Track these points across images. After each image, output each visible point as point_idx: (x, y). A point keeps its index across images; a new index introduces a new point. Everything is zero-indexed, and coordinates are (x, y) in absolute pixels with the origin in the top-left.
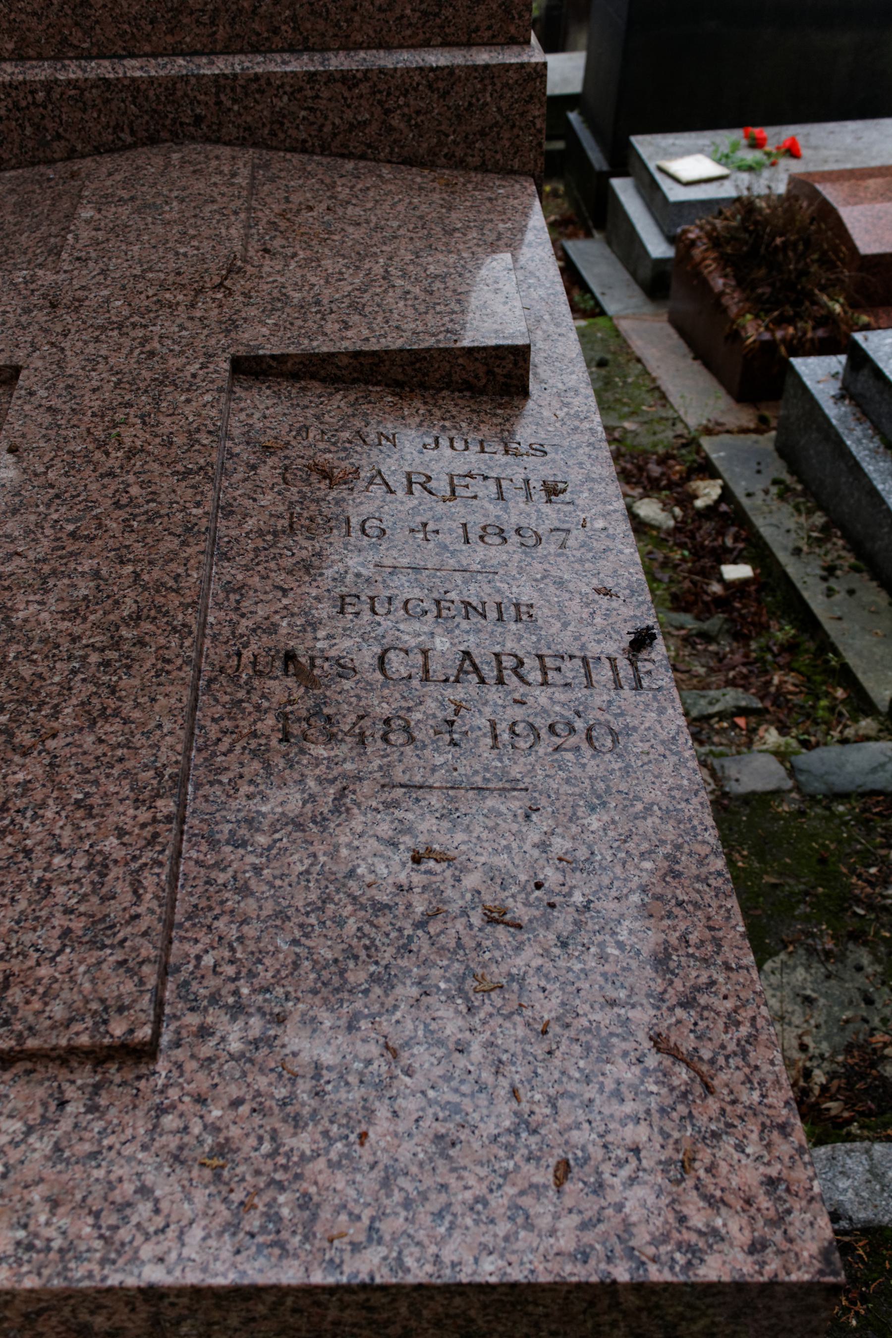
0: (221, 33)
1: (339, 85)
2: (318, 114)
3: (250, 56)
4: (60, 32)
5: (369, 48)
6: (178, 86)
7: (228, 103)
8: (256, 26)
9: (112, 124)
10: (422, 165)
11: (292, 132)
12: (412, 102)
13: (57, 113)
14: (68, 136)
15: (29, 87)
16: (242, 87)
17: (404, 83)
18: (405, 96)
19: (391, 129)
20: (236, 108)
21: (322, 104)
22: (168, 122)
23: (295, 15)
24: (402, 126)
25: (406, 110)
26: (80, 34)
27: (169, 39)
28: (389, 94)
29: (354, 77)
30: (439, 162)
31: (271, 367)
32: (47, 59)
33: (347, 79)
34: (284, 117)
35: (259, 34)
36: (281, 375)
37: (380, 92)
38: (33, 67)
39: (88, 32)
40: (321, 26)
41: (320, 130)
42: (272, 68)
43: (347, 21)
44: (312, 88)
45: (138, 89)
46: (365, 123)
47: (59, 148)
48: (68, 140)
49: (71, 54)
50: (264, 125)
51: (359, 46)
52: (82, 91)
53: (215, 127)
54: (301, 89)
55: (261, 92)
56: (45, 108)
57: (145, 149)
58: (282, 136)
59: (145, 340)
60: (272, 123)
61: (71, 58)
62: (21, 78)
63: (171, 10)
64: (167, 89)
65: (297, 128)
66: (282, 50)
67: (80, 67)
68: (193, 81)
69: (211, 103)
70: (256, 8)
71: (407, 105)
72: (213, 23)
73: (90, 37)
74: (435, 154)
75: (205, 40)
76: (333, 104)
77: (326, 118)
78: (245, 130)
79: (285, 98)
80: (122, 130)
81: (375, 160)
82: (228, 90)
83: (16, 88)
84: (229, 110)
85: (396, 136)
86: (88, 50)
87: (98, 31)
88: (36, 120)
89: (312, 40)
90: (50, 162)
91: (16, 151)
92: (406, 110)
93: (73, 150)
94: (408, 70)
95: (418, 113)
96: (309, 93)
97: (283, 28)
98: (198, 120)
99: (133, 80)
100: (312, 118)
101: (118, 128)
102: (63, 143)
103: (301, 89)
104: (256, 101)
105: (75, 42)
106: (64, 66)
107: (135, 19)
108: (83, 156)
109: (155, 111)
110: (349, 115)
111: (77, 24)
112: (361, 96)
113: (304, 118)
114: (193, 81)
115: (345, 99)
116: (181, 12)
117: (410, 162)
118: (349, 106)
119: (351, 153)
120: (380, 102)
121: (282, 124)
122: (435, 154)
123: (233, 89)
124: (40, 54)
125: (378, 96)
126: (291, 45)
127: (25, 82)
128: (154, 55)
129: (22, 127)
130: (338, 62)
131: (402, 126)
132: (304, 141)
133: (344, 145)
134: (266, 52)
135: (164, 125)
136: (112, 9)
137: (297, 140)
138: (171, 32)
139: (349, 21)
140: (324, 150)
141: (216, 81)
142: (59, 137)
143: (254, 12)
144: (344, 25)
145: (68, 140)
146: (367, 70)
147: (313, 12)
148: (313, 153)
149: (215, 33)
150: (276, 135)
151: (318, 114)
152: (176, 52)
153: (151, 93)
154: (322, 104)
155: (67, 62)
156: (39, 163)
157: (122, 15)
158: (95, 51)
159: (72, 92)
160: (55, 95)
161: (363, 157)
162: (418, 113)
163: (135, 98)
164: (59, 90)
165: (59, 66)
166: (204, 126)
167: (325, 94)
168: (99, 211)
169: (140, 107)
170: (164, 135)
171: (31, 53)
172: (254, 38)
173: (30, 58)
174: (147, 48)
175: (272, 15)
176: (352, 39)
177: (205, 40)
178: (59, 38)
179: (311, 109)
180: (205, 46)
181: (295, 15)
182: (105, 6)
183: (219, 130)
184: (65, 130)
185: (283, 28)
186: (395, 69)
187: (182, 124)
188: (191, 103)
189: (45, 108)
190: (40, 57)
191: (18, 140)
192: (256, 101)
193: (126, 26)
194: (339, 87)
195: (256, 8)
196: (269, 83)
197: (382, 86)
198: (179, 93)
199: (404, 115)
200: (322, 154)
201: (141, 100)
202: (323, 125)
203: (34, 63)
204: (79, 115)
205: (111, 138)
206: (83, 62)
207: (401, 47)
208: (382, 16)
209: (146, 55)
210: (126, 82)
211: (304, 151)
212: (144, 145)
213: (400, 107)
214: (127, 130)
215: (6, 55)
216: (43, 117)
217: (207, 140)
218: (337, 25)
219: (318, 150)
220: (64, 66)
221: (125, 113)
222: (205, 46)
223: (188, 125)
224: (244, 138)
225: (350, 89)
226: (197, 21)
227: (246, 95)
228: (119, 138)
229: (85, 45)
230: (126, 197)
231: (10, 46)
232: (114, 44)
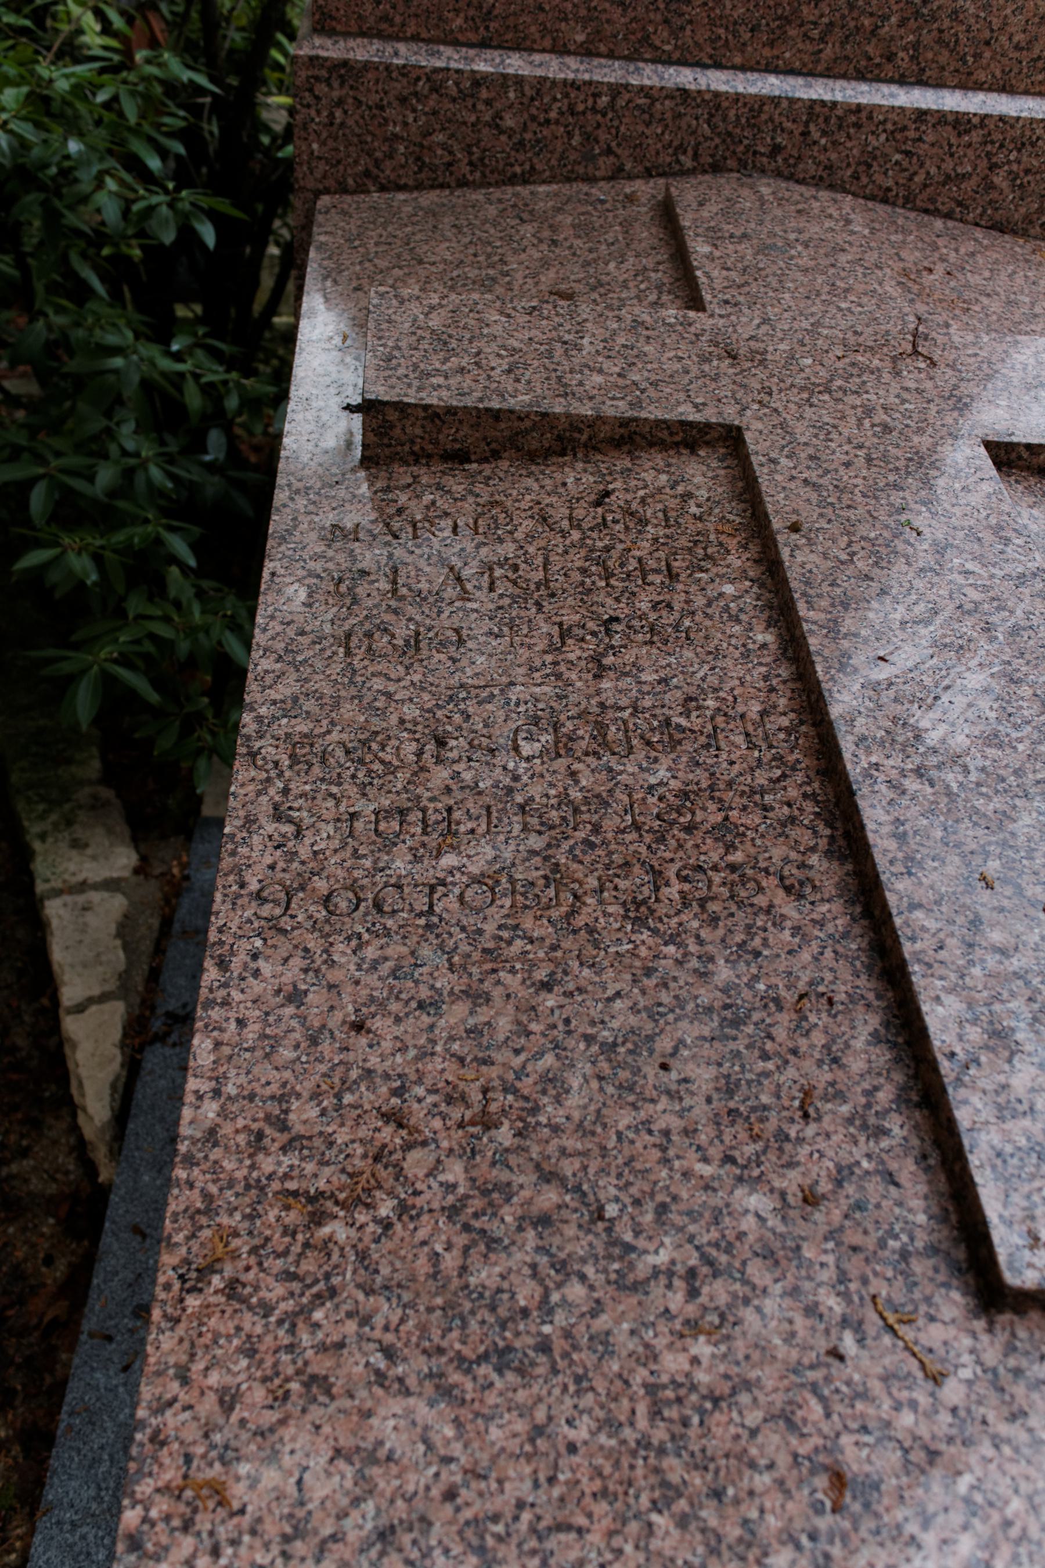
0: (828, 52)
1: (949, 128)
2: (915, 159)
3: (854, 83)
4: (644, 29)
5: (990, 90)
6: (766, 108)
7: (816, 135)
8: (870, 49)
9: (676, 143)
10: (1014, 232)
11: (879, 178)
12: (1025, 159)
13: (616, 123)
14: (619, 151)
15: (593, 89)
16: (839, 118)
17: (1023, 135)
18: (1019, 151)
19: (991, 187)
20: (823, 141)
21: (922, 149)
22: (741, 148)
23: (918, 42)
24: (1005, 185)
25: (1015, 167)
26: (665, 34)
27: (767, 52)
28: (1002, 146)
29: (969, 121)
30: (1032, 232)
31: (1020, 458)
32: (618, 58)
33: (960, 122)
34: (875, 158)
35: (870, 59)
36: (1028, 468)
37: (992, 142)
38: (601, 66)
39: (676, 32)
40: (944, 57)
41: (910, 179)
42: (877, 100)
43: (974, 56)
44: (917, 129)
45: (718, 107)
46: (964, 177)
47: (605, 164)
48: (617, 156)
49: (647, 56)
50: (849, 165)
51: (979, 87)
52: (654, 100)
53: (792, 161)
54: (905, 128)
55: (858, 126)
56: (604, 115)
57: (707, 177)
58: (865, 180)
59: (869, 412)
60: (859, 164)
61: (646, 61)
62: (587, 77)
63: (779, 18)
64: (751, 110)
65: (885, 174)
66: (891, 81)
67: (656, 72)
68: (785, 104)
69: (796, 133)
70: (877, 27)
71: (1019, 162)
72: (822, 40)
73: (677, 39)
74: (1031, 222)
75: (806, 58)
76: (935, 150)
77: (922, 165)
78: (826, 168)
79: (883, 137)
80: (685, 152)
81: (961, 221)
82: (821, 120)
83: (578, 89)
84: (815, 143)
85: (994, 195)
86: (670, 54)
87: (688, 32)
88: (589, 129)
89: (928, 73)
90: (591, 180)
91: (554, 162)
92: (1015, 167)
93: (621, 169)
94: (1032, 120)
95: (1027, 171)
96: (912, 134)
97: (901, 54)
98: (776, 149)
99: (717, 94)
100: (905, 164)
101: (681, 148)
102: (612, 159)
103: (905, 128)
104: (849, 137)
105: (657, 43)
106: (637, 69)
107: (735, 23)
108: (630, 178)
109: (729, 134)
110: (948, 165)
111: (666, 21)
112: (970, 145)
113: (897, 163)
114: (785, 104)
115: (950, 146)
116: (789, 22)
117: (1000, 227)
118: (952, 155)
119: (937, 210)
120: (989, 155)
121: (870, 166)
122: (1031, 222)
123: (827, 120)
124: (612, 51)
125: (989, 148)
126: (903, 76)
127: (590, 83)
128: (743, 68)
129: (570, 135)
130: (952, 101)
131: (1005, 185)
132: (889, 189)
133: (932, 200)
134: (872, 80)
135: (734, 152)
136: (713, 9)
137: (880, 187)
138: (771, 44)
139: (977, 56)
140: (909, 202)
141: (811, 107)
142: (609, 151)
143: (873, 33)
144: (970, 59)
145: (617, 156)
146: (986, 116)
147: (940, 41)
148: (894, 204)
149: (821, 51)
150: (858, 179)
151: (915, 159)
152: (770, 68)
153: (732, 113)
154: (922, 149)
155: (641, 65)
156: (576, 179)
157: (721, 17)
158: (676, 55)
159: (641, 101)
160: (621, 102)
161: (948, 216)
162: (1027, 171)
163: (711, 115)
164: (627, 96)
165: (632, 68)
166: (779, 159)
167: (930, 138)
168: (715, 246)
169: (713, 128)
170: (731, 163)
171: (603, 48)
172: (863, 63)
173: (599, 55)
174: (738, 60)
175: (892, 39)
176: (974, 77)
177: (806, 58)
178: (639, 35)
179: (908, 153)
180: (804, 65)
181: (918, 42)
182: (705, 4)
183: (795, 165)
184: (619, 145)
185: (901, 54)
186: (1018, 118)
187: (755, 153)
188: (774, 130)
189: (604, 115)
190: (611, 55)
191: (560, 150)
192: (849, 137)
193: (721, 31)
194: (948, 132)
195: (877, 27)
196: (870, 118)
197: (997, 136)
198: (764, 117)
199: (1010, 172)
200: (903, 207)
201: (717, 119)
202: (915, 173)
203: (603, 61)
204: (641, 128)
205: (668, 159)
206: (660, 67)
207: (1026, 93)
208: (1017, 55)
209: (734, 67)
210: (707, 97)
211: (885, 201)
212: (705, 172)
213: (1009, 162)
214: (690, 152)
215: (572, 48)
216: (599, 126)
217: (779, 174)
218: (963, 59)
219: (900, 201)
220: (637, 69)
221: (694, 133)
222: (804, 65)
223: (762, 155)
224: (821, 178)
225: (959, 135)
226: (805, 35)
227: (840, 127)
228: (678, 161)
229: (667, 48)
230: (738, 233)
231: (580, 38)
232: (701, 50)
